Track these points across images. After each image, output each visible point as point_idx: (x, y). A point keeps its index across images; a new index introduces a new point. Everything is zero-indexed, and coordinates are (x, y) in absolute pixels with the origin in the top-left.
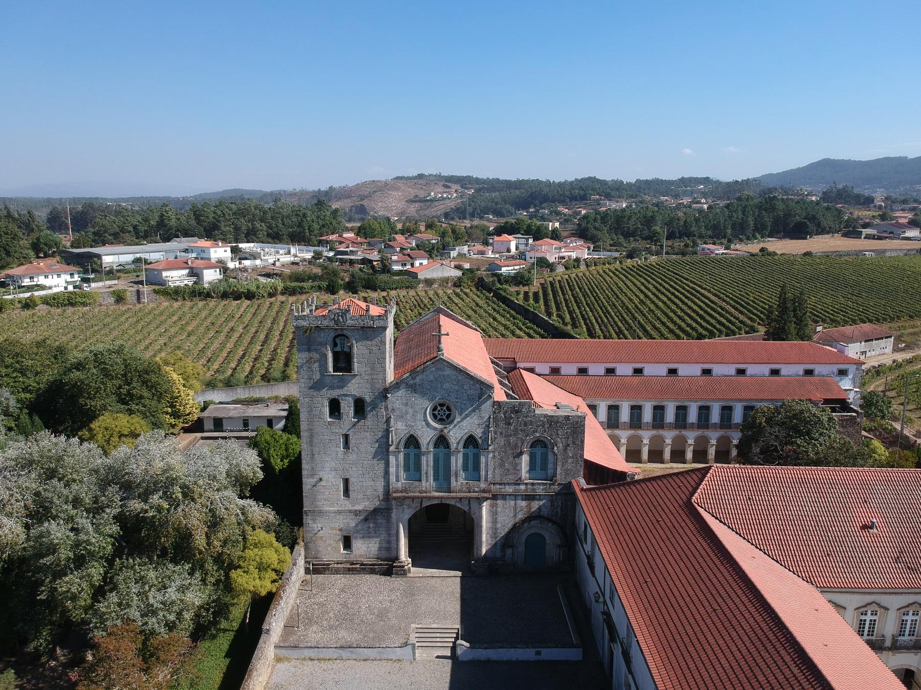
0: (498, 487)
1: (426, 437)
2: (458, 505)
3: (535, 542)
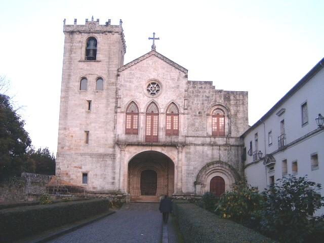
0: (191, 139)
1: (143, 101)
2: (163, 152)
3: (218, 183)
